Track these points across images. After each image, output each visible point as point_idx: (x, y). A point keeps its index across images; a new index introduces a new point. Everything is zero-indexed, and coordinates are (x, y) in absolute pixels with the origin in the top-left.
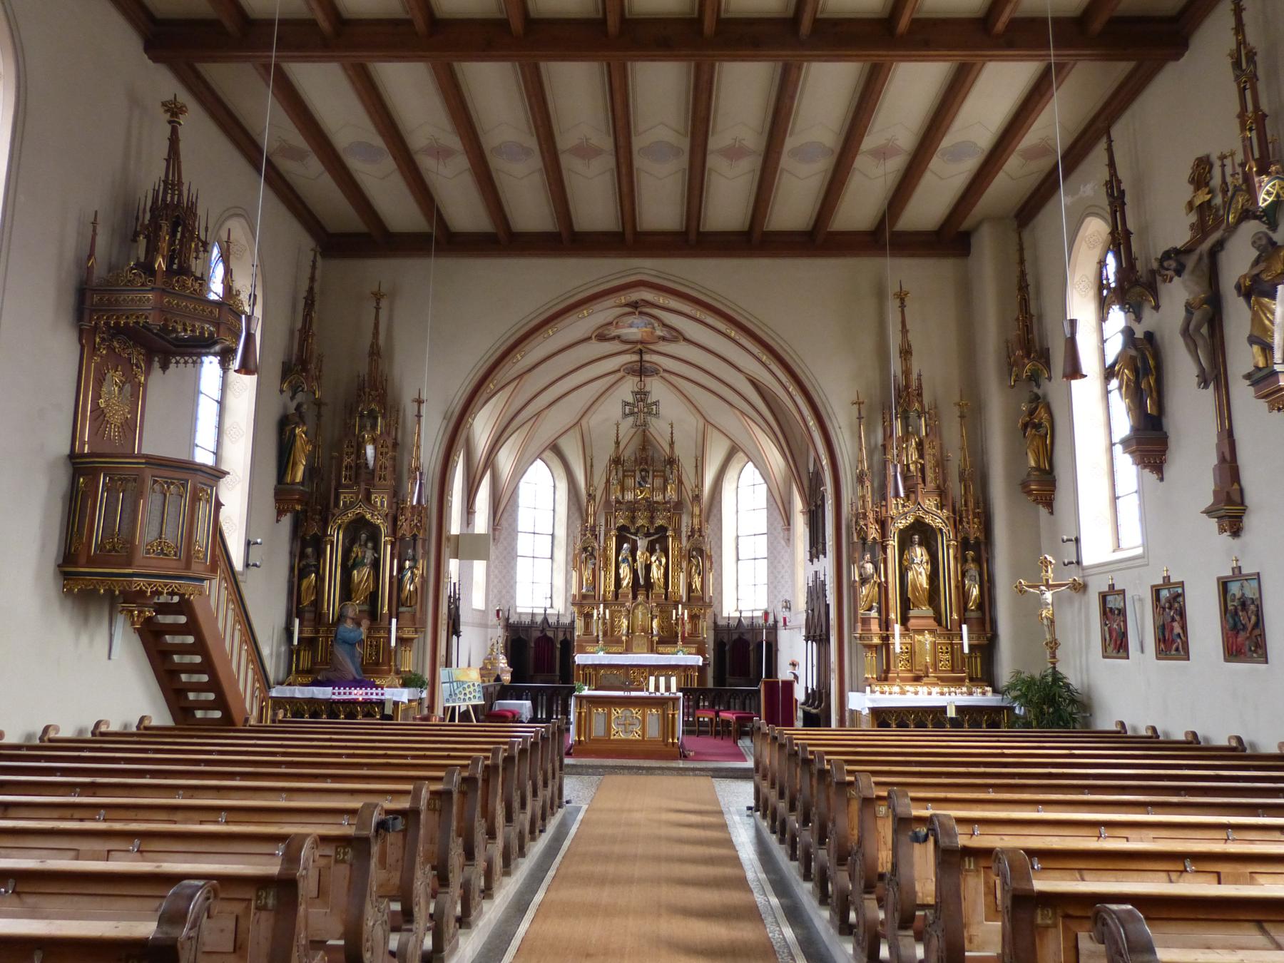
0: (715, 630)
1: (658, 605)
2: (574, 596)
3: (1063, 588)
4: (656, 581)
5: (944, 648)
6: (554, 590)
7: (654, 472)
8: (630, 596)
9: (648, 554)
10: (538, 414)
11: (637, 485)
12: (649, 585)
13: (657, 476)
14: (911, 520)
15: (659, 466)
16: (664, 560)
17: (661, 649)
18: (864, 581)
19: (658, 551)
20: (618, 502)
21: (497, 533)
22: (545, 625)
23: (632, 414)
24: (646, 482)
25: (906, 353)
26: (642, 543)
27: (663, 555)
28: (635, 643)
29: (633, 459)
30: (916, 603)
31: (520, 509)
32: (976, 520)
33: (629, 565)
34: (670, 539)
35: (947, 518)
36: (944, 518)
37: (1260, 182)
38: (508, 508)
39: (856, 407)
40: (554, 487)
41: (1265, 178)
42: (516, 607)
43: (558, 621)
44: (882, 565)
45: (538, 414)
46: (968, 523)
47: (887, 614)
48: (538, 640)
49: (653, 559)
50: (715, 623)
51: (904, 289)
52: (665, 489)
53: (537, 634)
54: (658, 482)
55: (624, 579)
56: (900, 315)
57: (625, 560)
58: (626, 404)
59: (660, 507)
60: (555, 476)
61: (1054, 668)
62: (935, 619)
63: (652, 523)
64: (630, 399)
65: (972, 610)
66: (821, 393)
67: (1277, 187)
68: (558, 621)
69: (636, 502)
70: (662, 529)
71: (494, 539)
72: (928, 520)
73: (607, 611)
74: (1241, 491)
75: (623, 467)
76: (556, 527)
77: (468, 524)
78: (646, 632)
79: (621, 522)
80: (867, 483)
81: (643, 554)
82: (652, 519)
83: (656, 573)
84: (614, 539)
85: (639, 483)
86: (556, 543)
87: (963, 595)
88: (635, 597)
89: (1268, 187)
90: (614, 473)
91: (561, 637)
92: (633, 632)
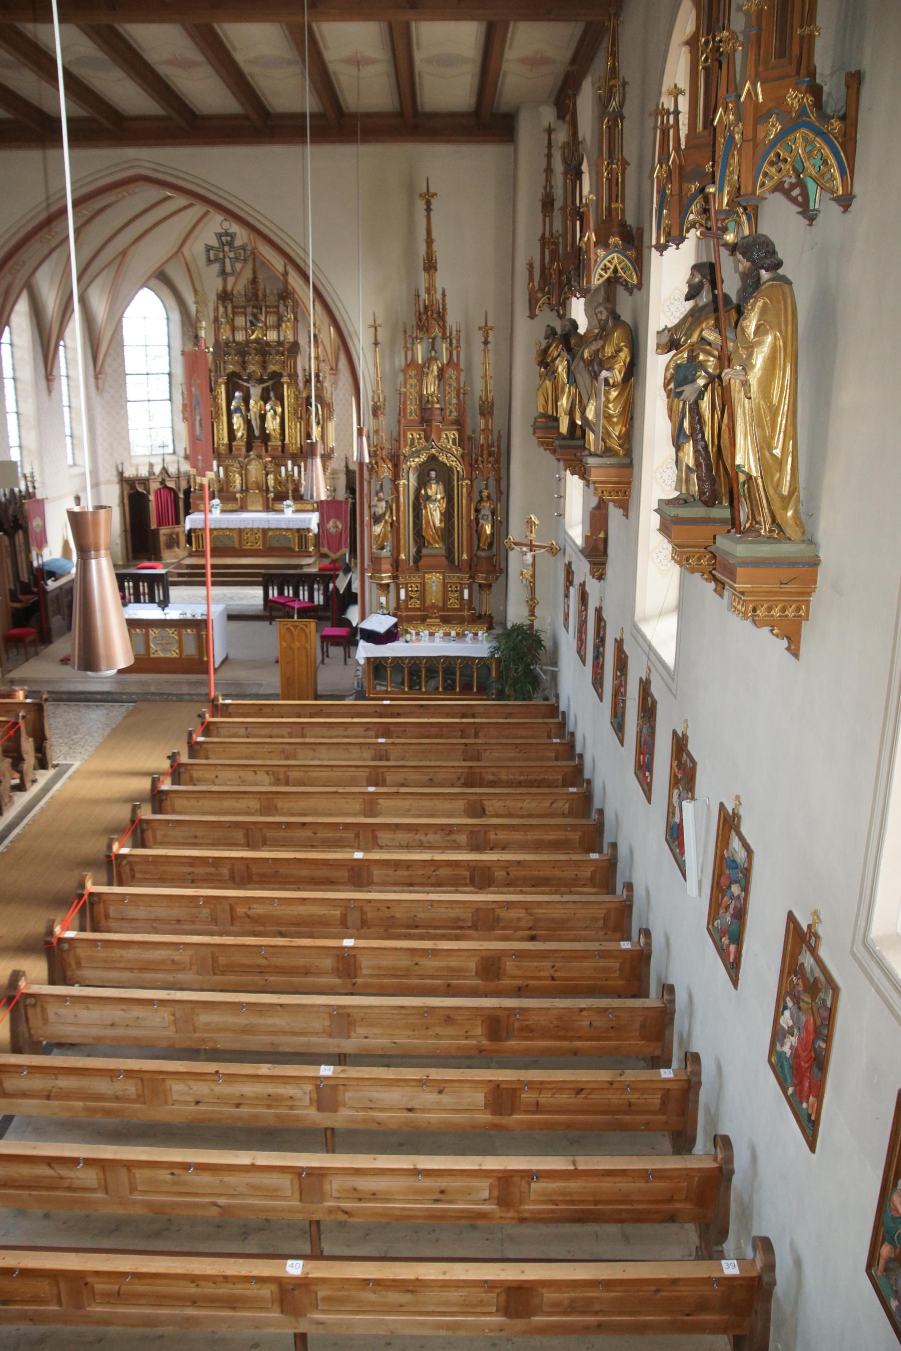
0: (347, 475)
1: (273, 458)
2: (185, 449)
3: (542, 550)
4: (273, 433)
5: (454, 586)
6: (176, 434)
7: (267, 307)
8: (244, 450)
9: (262, 403)
10: (124, 253)
11: (249, 324)
12: (265, 438)
13: (271, 312)
14: (423, 458)
15: (272, 300)
16: (279, 410)
17: (278, 506)
18: (377, 519)
19: (273, 399)
20: (227, 344)
21: (100, 382)
22: (165, 475)
23: (217, 260)
24: (258, 320)
25: (430, 266)
26: (256, 392)
27: (279, 403)
28: (249, 502)
29: (243, 292)
30: (431, 541)
31: (127, 350)
32: (491, 459)
33: (242, 416)
34: (285, 386)
35: (462, 456)
36: (459, 456)
37: (596, 254)
38: (111, 351)
39: (373, 330)
40: (168, 319)
41: (601, 252)
42: (130, 457)
43: (179, 470)
44: (394, 506)
45: (124, 253)
46: (482, 462)
47: (398, 554)
48: (158, 493)
49: (268, 407)
50: (347, 467)
51: (432, 190)
52: (278, 327)
53: (155, 486)
54: (272, 320)
55: (238, 429)
56: (425, 221)
57: (238, 409)
58: (209, 249)
59: (273, 352)
60: (167, 306)
61: (531, 626)
62: (447, 558)
63: (264, 368)
64: (214, 243)
65: (484, 550)
66: (342, 310)
67: (616, 261)
68: (179, 470)
69: (248, 342)
70: (276, 376)
71: (97, 388)
72: (442, 458)
73: (221, 469)
74: (606, 540)
75: (232, 302)
76: (172, 365)
77: (50, 391)
78: (261, 490)
79: (231, 368)
80: (381, 418)
81: (256, 403)
82: (264, 365)
83: (272, 425)
84: (223, 387)
85: (251, 322)
86: (173, 382)
87: (479, 531)
88: (249, 448)
89: (605, 262)
90: (221, 310)
91: (184, 485)
92: (247, 490)
